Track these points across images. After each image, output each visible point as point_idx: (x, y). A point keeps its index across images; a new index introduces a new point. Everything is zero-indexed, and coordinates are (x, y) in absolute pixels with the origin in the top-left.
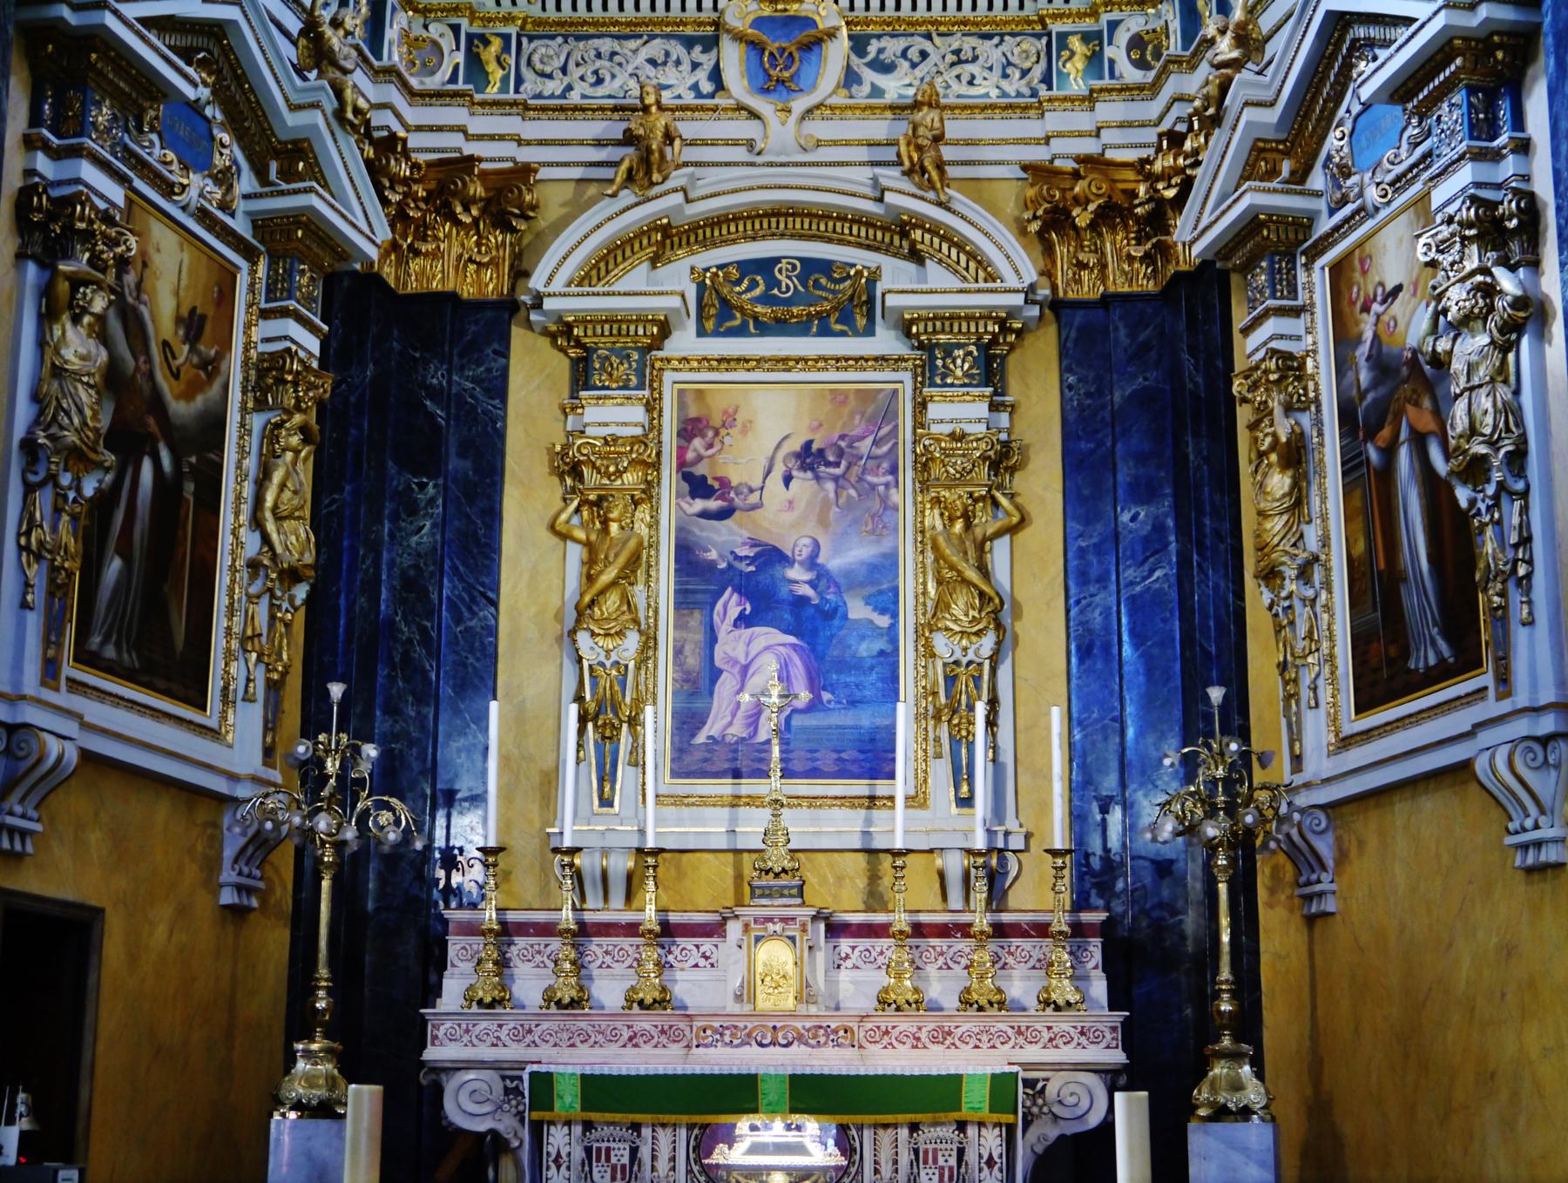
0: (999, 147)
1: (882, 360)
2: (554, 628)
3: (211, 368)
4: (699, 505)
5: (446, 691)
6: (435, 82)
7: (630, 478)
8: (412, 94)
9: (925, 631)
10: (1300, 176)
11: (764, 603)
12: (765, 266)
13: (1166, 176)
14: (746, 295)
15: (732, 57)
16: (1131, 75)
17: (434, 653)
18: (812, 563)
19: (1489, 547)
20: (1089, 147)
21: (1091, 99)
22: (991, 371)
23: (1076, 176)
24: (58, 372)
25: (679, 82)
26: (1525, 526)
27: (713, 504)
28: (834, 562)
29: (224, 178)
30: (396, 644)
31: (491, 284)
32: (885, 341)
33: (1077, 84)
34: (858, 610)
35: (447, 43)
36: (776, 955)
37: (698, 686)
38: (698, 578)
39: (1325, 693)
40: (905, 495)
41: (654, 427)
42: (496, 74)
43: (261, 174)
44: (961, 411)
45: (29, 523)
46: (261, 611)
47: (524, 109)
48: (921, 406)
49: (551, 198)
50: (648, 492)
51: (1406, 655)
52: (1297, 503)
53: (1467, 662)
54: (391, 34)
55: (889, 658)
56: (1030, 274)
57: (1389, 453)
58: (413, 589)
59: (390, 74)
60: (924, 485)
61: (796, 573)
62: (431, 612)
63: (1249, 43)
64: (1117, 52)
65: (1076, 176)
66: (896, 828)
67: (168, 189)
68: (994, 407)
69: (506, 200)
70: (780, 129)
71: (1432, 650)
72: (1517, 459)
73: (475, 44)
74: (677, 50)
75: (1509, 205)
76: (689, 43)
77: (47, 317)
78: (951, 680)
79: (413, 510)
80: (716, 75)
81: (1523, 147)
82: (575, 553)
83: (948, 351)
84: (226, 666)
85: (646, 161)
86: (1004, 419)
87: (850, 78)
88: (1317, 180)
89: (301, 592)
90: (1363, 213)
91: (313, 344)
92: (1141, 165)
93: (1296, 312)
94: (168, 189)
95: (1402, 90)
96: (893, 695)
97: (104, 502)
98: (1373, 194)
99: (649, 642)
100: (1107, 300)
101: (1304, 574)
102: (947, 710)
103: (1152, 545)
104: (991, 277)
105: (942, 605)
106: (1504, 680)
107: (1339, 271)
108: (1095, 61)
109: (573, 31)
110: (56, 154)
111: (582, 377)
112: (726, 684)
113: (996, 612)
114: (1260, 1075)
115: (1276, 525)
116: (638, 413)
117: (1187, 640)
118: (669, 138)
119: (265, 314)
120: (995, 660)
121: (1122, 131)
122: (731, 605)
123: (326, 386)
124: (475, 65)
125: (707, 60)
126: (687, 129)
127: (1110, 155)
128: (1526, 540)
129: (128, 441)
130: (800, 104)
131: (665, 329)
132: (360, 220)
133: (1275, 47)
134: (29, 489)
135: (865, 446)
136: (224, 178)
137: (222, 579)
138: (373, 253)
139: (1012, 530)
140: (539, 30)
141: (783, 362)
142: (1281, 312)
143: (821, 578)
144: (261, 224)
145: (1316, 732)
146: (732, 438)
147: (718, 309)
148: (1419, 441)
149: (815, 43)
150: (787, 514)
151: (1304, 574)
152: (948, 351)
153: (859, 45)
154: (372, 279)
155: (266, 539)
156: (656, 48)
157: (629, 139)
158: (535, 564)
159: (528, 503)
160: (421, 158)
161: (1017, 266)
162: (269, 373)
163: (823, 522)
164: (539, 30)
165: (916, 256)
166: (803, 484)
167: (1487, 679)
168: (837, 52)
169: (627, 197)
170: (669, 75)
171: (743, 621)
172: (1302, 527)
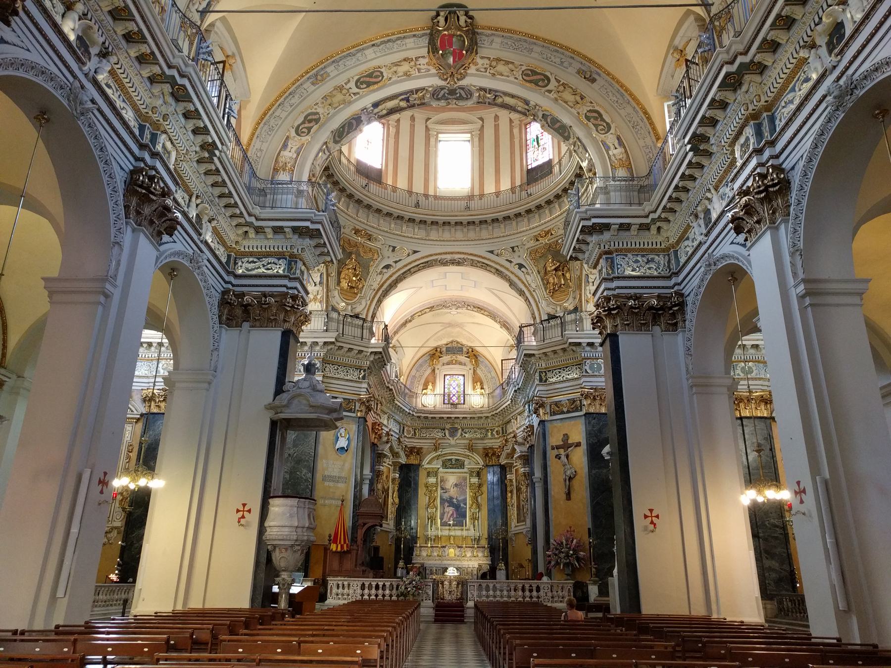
0: (480, 445)
9: (470, 508)
14: (448, 464)
15: (447, 432)
22: (478, 474)
25: (440, 435)
30: (405, 508)
31: (416, 462)
32: (465, 470)
33: (490, 436)
34: (462, 505)
36: (452, 550)
38: (443, 501)
40: (468, 490)
44: (475, 480)
49: (424, 451)
50: (437, 490)
63: (506, 441)
66: (465, 533)
70: (452, 442)
84: (389, 516)
95: (520, 457)
96: (465, 517)
102: (474, 518)
103: (498, 498)
113: (479, 506)
114: (506, 565)
121: (494, 442)
122: (447, 504)
132: (403, 460)
143: (458, 501)
145: (513, 525)
147: (445, 466)
149: (456, 430)
150: (453, 492)
158: (423, 498)
159: (422, 491)
161: (481, 462)
162: (394, 480)
168: (460, 431)
172: (512, 500)
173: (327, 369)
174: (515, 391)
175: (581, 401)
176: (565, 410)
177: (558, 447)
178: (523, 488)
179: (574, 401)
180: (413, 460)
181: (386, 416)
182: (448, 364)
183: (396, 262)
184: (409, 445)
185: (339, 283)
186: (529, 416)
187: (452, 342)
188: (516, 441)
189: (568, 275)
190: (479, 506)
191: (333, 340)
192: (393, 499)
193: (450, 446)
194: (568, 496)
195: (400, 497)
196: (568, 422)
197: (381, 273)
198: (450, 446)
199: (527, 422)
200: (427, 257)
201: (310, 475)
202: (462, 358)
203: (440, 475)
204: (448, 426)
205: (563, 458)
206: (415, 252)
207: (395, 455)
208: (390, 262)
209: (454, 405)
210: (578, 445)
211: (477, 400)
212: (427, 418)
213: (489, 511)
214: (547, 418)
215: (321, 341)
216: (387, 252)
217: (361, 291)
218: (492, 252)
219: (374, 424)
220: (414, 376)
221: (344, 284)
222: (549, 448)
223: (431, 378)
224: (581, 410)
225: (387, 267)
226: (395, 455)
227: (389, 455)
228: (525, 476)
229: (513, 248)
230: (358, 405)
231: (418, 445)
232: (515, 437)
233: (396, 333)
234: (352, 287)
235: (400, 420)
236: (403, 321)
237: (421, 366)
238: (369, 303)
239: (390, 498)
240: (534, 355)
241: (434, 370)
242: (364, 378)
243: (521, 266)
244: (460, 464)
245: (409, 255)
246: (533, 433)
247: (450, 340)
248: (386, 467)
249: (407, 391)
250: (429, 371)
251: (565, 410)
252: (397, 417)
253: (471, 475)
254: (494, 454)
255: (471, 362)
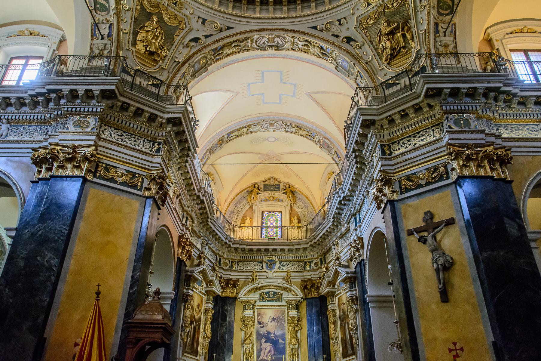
1: (283, 306)
2: (240, 343)
3: (200, 311)
4: (260, 325)
5: (226, 352)
6: (227, 268)
7: (251, 322)
8: (224, 270)
9: (289, 344)
10: (334, 286)
11: (268, 339)
12: (268, 293)
13: (318, 283)
14: (266, 297)
15: (264, 265)
16: (315, 268)
17: (225, 347)
18: (274, 334)
19: (354, 340)
20: (309, 277)
21: (309, 271)
22: (297, 307)
23: (308, 281)
24: (186, 316)
25: (258, 267)
26: (358, 338)
27: (262, 326)
28: (277, 334)
29: (202, 286)
31: (234, 295)
33: (308, 269)
34: (280, 341)
35: (228, 263)
37: (259, 351)
38: (260, 336)
39: (339, 355)
40: (286, 324)
41: (254, 315)
42: (234, 267)
43: (207, 286)
44: (293, 313)
45: (181, 336)
46: (204, 343)
47: (237, 271)
48: (288, 312)
49: (240, 283)
51: (347, 351)
52: (335, 330)
53: (353, 354)
54: (222, 262)
55: (284, 347)
56: (302, 296)
57: (345, 324)
58: (223, 337)
59: (222, 268)
60: (289, 323)
61: (272, 335)
62: (225, 341)
64: (313, 265)
65: (308, 281)
67: (197, 289)
68: (298, 312)
69: (235, 284)
70: (270, 274)
71: (350, 352)
72: (357, 329)
73: (232, 262)
74: (257, 263)
75: (354, 297)
76: (259, 262)
77: (185, 309)
78: (292, 351)
79: (223, 326)
80: (262, 267)
81: (356, 290)
82: (243, 332)
83: (292, 305)
84: (200, 351)
85: (253, 279)
86: (299, 314)
87: (279, 267)
88: (336, 287)
89: (209, 340)
90: (340, 293)
91: (211, 306)
92: (316, 280)
93: (334, 304)
94: (197, 289)
95: (344, 281)
96: (284, 353)
97: (188, 332)
98: (342, 291)
99: (253, 345)
100: (312, 298)
101: (336, 339)
104: (297, 295)
105: (291, 341)
106: (356, 357)
107: (339, 299)
108: (310, 265)
109: (244, 261)
110: (186, 289)
111: (245, 308)
112: (263, 351)
113: (298, 341)
115: (332, 332)
116: (252, 313)
117: (323, 346)
118: (256, 276)
119: (206, 303)
120: (298, 348)
121: (314, 275)
122: (264, 340)
123: (213, 311)
124: (232, 266)
125: (261, 265)
126: (258, 274)
127: (312, 279)
128: (358, 339)
129: (192, 323)
130: (273, 271)
131: (256, 302)
132: (217, 289)
133: (331, 269)
134: (181, 331)
135: (281, 317)
136: (202, 286)
137: (200, 339)
138: (220, 294)
139: (300, 330)
140: (240, 261)
141: (270, 306)
142: (332, 304)
143: (276, 336)
144: (206, 291)
146: (264, 316)
147: (262, 299)
148: (348, 323)
149: (274, 262)
150: (271, 327)
151: (336, 339)
152: (292, 305)
153: (280, 263)
154: (219, 295)
155: (205, 333)
156: (255, 263)
157: (251, 276)
159: (237, 326)
160: (225, 278)
161: (300, 294)
163: (276, 328)
164: (240, 261)
165: (287, 291)
166: (273, 323)
167: (354, 357)
168: (278, 264)
169: (251, 284)
170: (256, 267)
171: (265, 342)
172: (336, 333)
173: (107, 132)
174: (340, 202)
175: (445, 167)
176: (423, 182)
177: (418, 230)
178: (351, 314)
179: (436, 169)
180: (229, 293)
181: (200, 240)
182: (266, 200)
183: (206, 37)
184: (226, 277)
185: (134, 44)
186: (356, 230)
187: (269, 179)
188: (340, 264)
189: (408, 36)
190: (298, 341)
191: (113, 87)
192: (205, 332)
193: (267, 278)
194: (445, 296)
195: (212, 330)
196: (428, 197)
197: (187, 46)
198: (267, 278)
199: (354, 237)
200: (241, 33)
201: (55, 261)
202: (279, 195)
203: (256, 308)
204: (266, 259)
205: (430, 240)
206: (229, 28)
207: (210, 283)
208: (200, 35)
209: (273, 239)
210: (450, 222)
211: (295, 234)
212: (243, 250)
213: (309, 346)
214: (396, 197)
215: (96, 88)
216: (195, 24)
217: (163, 60)
218: (315, 28)
219: (181, 237)
220: (233, 212)
221: (140, 46)
222: (403, 235)
223: (249, 214)
224: (448, 178)
225: (196, 40)
226: (210, 283)
227: (200, 277)
228: (352, 300)
229: (339, 21)
230: (146, 183)
231: (234, 278)
232: (338, 259)
233: (211, 151)
234: (152, 53)
235: (216, 250)
236: (219, 137)
237: (239, 201)
238: (171, 75)
239: (202, 330)
240: (373, 122)
241: (252, 207)
242: (158, 151)
243: (349, 40)
244: (277, 298)
245: (221, 30)
246: (362, 247)
247: (268, 176)
248: (197, 294)
249: (225, 223)
250: (247, 207)
251: (423, 182)
252: (212, 246)
253: (289, 308)
254: (313, 286)
255: (288, 197)
